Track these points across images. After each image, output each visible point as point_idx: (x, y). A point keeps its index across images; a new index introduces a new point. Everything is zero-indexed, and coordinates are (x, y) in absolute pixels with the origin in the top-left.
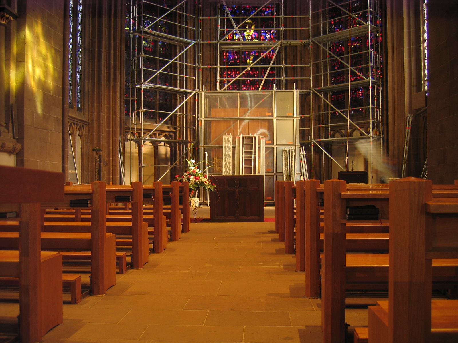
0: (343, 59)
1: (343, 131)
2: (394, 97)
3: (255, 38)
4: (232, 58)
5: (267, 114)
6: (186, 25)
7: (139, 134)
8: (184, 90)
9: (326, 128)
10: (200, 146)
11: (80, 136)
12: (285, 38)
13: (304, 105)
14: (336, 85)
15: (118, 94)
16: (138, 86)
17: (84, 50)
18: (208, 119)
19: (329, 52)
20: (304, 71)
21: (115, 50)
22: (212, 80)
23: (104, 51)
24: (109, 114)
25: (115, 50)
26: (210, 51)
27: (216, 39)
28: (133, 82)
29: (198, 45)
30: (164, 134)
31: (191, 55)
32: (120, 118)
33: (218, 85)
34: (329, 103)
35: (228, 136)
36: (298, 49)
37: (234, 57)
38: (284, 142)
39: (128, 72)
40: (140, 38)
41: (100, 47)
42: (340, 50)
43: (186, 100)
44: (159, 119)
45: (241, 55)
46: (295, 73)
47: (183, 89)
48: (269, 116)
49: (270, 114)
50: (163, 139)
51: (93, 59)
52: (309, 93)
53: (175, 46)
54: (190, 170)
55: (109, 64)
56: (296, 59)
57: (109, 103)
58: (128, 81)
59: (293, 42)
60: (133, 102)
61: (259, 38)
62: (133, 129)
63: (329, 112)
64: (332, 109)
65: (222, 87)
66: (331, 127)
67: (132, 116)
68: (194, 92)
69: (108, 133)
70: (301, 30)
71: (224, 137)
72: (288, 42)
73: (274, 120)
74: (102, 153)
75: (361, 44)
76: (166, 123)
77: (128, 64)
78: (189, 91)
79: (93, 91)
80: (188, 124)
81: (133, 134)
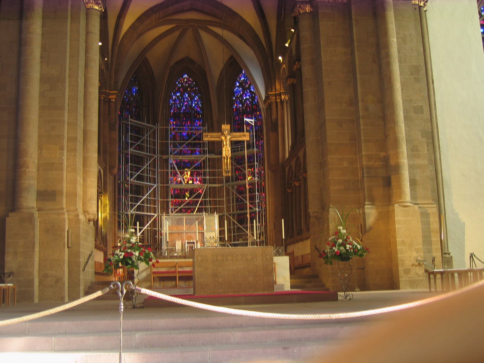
0: (243, 197)
1: (244, 237)
2: (269, 219)
3: (190, 180)
4: (176, 193)
5: (201, 229)
6: (150, 174)
8: (149, 214)
9: (234, 236)
12: (209, 183)
13: (221, 222)
14: (240, 212)
19: (235, 192)
20: (221, 203)
22: (165, 207)
26: (164, 189)
27: (168, 183)
33: (170, 210)
34: (235, 222)
35: (179, 242)
36: (217, 189)
37: (178, 192)
42: (241, 190)
45: (182, 190)
46: (215, 202)
48: (201, 230)
49: (202, 229)
52: (224, 215)
53: (143, 187)
56: (216, 194)
59: (214, 185)
61: (193, 180)
63: (236, 227)
64: (237, 225)
65: (172, 212)
66: (237, 235)
68: (156, 215)
70: (218, 179)
71: (176, 242)
72: (211, 185)
75: (253, 186)
78: (153, 214)
80: (151, 234)
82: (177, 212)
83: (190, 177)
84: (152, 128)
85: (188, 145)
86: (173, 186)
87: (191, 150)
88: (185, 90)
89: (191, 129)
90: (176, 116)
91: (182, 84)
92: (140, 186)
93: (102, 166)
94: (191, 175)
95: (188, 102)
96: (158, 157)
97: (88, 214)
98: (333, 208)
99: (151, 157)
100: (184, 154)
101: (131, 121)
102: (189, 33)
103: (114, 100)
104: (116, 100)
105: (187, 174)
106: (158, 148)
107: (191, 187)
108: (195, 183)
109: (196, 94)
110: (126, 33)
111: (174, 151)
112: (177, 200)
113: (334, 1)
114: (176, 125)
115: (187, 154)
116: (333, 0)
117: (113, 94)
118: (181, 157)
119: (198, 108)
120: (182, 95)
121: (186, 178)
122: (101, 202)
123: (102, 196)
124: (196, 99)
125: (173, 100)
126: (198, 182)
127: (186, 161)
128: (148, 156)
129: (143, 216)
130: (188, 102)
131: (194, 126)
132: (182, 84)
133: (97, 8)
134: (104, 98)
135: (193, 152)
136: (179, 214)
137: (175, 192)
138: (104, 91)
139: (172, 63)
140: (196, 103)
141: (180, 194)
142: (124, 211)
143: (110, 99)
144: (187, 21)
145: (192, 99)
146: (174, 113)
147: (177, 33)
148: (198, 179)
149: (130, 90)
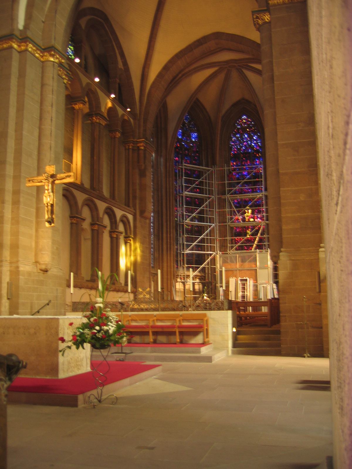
3: (252, 218)
7: (184, 278)
10: (217, 285)
11: (153, 281)
15: (172, 258)
16: (183, 252)
17: (154, 235)
18: (221, 270)
21: (170, 234)
23: (165, 235)
24: (167, 269)
25: (170, 234)
28: (180, 250)
29: (216, 226)
30: (198, 277)
31: (211, 233)
32: (174, 270)
35: (233, 279)
38: (264, 282)
39: (177, 245)
40: (183, 225)
41: (162, 234)
43: (211, 257)
44: (195, 269)
47: (208, 251)
48: (255, 267)
50: (198, 281)
51: (159, 240)
53: (204, 227)
54: (204, 298)
55: (167, 242)
57: (167, 263)
58: (177, 249)
60: (180, 261)
61: (253, 218)
62: (181, 276)
67: (180, 268)
69: (167, 279)
73: (258, 270)
74: (164, 290)
76: (199, 272)
77: (177, 240)
79: (159, 257)
81: (181, 279)
82: (236, 249)
83: (251, 215)
84: (209, 170)
85: (247, 183)
86: (229, 223)
87: (251, 188)
88: (244, 130)
89: (251, 168)
90: (236, 157)
91: (241, 125)
92: (201, 227)
93: (130, 212)
94: (252, 213)
95: (247, 142)
96: (215, 198)
97: (40, 264)
98: (285, 251)
99: (209, 198)
100: (245, 193)
101: (186, 166)
102: (235, 74)
103: (142, 148)
104: (144, 147)
105: (248, 212)
106: (215, 189)
107: (251, 225)
108: (256, 220)
109: (255, 134)
110: (154, 83)
111: (230, 191)
112: (238, 237)
113: (290, 1)
114: (237, 165)
115: (249, 192)
116: (288, 1)
117: (141, 142)
118: (239, 196)
119: (257, 147)
120: (241, 137)
121: (247, 216)
122: (130, 245)
123: (130, 240)
124: (254, 138)
125: (233, 142)
126: (258, 219)
127: (246, 199)
128: (206, 197)
129: (204, 254)
130: (247, 142)
131: (254, 165)
132: (241, 125)
133: (52, 59)
134: (133, 146)
135: (254, 191)
136: (239, 252)
137: (237, 230)
138: (133, 139)
139: (227, 106)
140: (255, 142)
141: (242, 232)
142: (182, 251)
143: (138, 147)
144: (227, 62)
145: (251, 138)
146: (234, 154)
147: (222, 76)
148: (259, 216)
149: (190, 136)
